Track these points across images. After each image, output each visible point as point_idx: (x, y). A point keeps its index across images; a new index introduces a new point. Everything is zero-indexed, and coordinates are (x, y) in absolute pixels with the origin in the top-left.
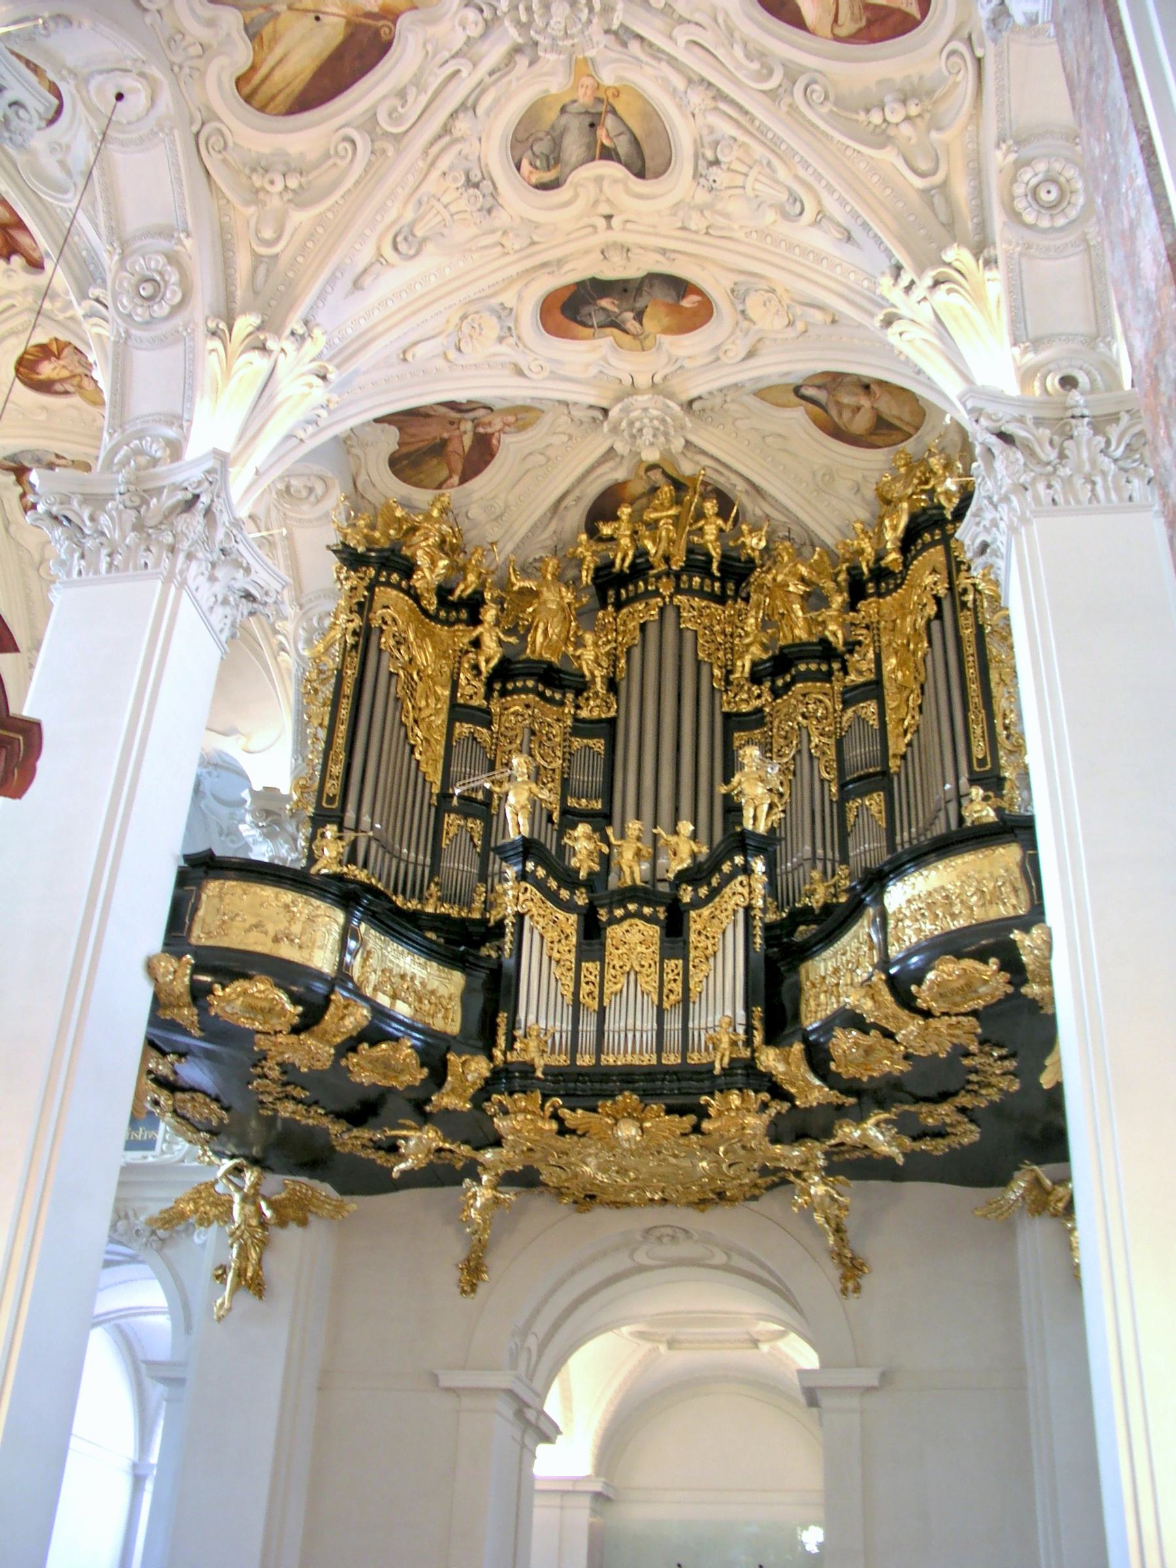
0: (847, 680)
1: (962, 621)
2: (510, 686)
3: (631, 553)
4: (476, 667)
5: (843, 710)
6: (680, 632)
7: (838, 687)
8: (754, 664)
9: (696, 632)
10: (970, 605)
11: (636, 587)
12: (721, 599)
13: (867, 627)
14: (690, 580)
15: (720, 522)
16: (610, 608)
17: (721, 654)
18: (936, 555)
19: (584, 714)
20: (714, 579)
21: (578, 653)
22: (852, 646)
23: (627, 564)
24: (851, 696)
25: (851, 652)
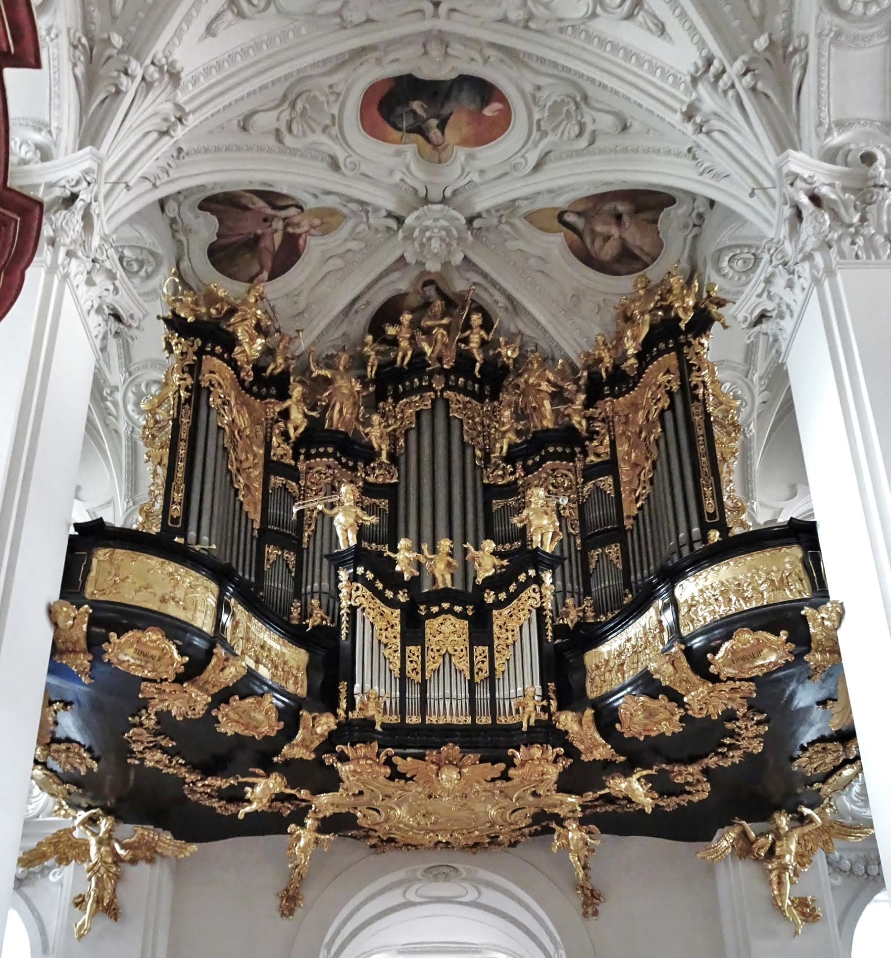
0: (588, 460)
1: (693, 410)
2: (313, 451)
3: (410, 353)
4: (285, 434)
5: (584, 483)
6: (448, 419)
7: (579, 465)
8: (510, 447)
9: (461, 421)
10: (700, 396)
11: (412, 382)
12: (480, 398)
13: (603, 421)
14: (457, 380)
15: (482, 333)
16: (390, 400)
17: (480, 439)
18: (671, 359)
19: (371, 479)
20: (475, 380)
21: (367, 430)
22: (592, 434)
23: (406, 362)
24: (590, 472)
25: (591, 440)
